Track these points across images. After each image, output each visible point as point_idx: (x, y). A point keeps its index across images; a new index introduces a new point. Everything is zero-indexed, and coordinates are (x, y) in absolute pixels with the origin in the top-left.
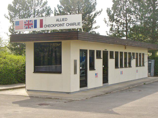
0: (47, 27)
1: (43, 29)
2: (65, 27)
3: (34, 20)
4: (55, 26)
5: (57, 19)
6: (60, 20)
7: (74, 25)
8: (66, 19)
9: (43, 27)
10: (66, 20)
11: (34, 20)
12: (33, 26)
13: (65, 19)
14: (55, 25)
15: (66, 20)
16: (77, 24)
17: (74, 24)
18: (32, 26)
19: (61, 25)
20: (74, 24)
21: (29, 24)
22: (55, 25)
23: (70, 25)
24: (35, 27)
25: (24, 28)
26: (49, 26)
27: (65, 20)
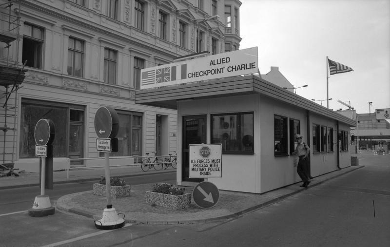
0: (193, 76)
1: (184, 81)
2: (225, 74)
3: (172, 67)
4: (208, 73)
5: (212, 61)
6: (216, 63)
7: (243, 68)
9: (186, 78)
10: (228, 59)
11: (172, 67)
12: (171, 77)
13: (225, 59)
14: (206, 73)
16: (248, 67)
17: (242, 67)
18: (169, 78)
19: (217, 71)
20: (243, 66)
21: (163, 75)
23: (234, 70)
24: (174, 78)
25: (155, 82)
26: (195, 75)
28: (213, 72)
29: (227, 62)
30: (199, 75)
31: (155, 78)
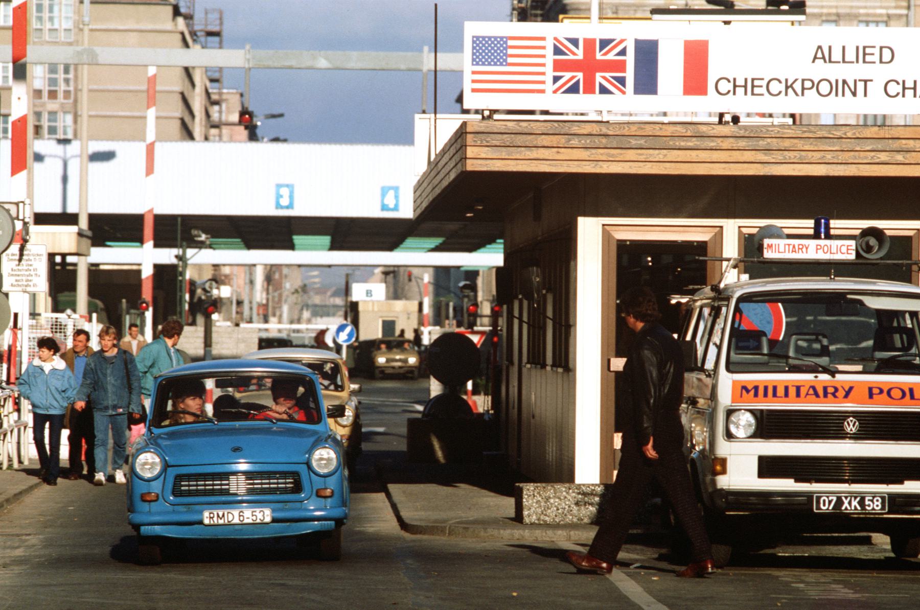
0: (740, 91)
3: (637, 42)
4: (803, 89)
5: (820, 47)
8: (887, 54)
10: (887, 55)
12: (630, 75)
13: (876, 51)
14: (798, 86)
15: (887, 55)
18: (622, 81)
19: (840, 87)
21: (589, 66)
24: (647, 82)
25: (549, 86)
26: (750, 86)
27: (876, 58)
28: (824, 88)
29: (881, 62)
30: (763, 90)
31: (550, 73)
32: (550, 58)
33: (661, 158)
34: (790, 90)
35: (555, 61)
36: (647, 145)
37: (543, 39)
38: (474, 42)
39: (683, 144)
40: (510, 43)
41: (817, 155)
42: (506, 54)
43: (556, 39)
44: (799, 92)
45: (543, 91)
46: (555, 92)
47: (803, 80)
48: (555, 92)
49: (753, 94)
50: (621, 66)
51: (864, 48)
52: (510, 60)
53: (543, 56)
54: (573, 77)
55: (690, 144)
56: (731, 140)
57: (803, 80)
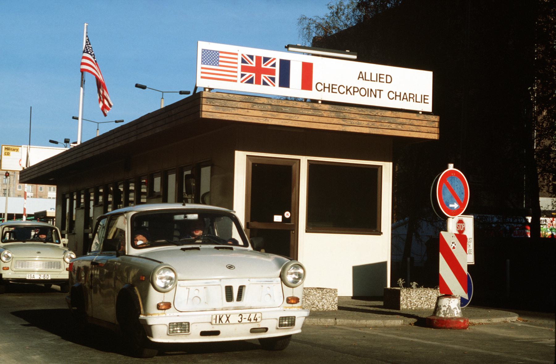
0: (327, 90)
4: (354, 92)
5: (361, 72)
7: (411, 99)
8: (389, 79)
10: (389, 80)
12: (277, 77)
13: (385, 77)
14: (352, 90)
15: (389, 80)
16: (419, 99)
17: (410, 98)
18: (273, 79)
19: (369, 92)
21: (258, 70)
22: (352, 88)
23: (398, 98)
24: (285, 82)
25: (239, 79)
26: (331, 88)
27: (384, 80)
28: (363, 92)
29: (387, 82)
30: (336, 91)
32: (240, 64)
33: (296, 118)
34: (348, 92)
35: (242, 66)
36: (289, 111)
37: (237, 54)
38: (203, 52)
39: (306, 112)
40: (221, 54)
41: (365, 123)
42: (218, 60)
43: (242, 55)
44: (352, 93)
45: (236, 81)
46: (242, 82)
47: (354, 87)
48: (242, 82)
49: (332, 92)
50: (273, 72)
51: (380, 75)
52: (220, 63)
53: (236, 63)
54: (250, 75)
55: (310, 113)
56: (329, 112)
57: (354, 87)
